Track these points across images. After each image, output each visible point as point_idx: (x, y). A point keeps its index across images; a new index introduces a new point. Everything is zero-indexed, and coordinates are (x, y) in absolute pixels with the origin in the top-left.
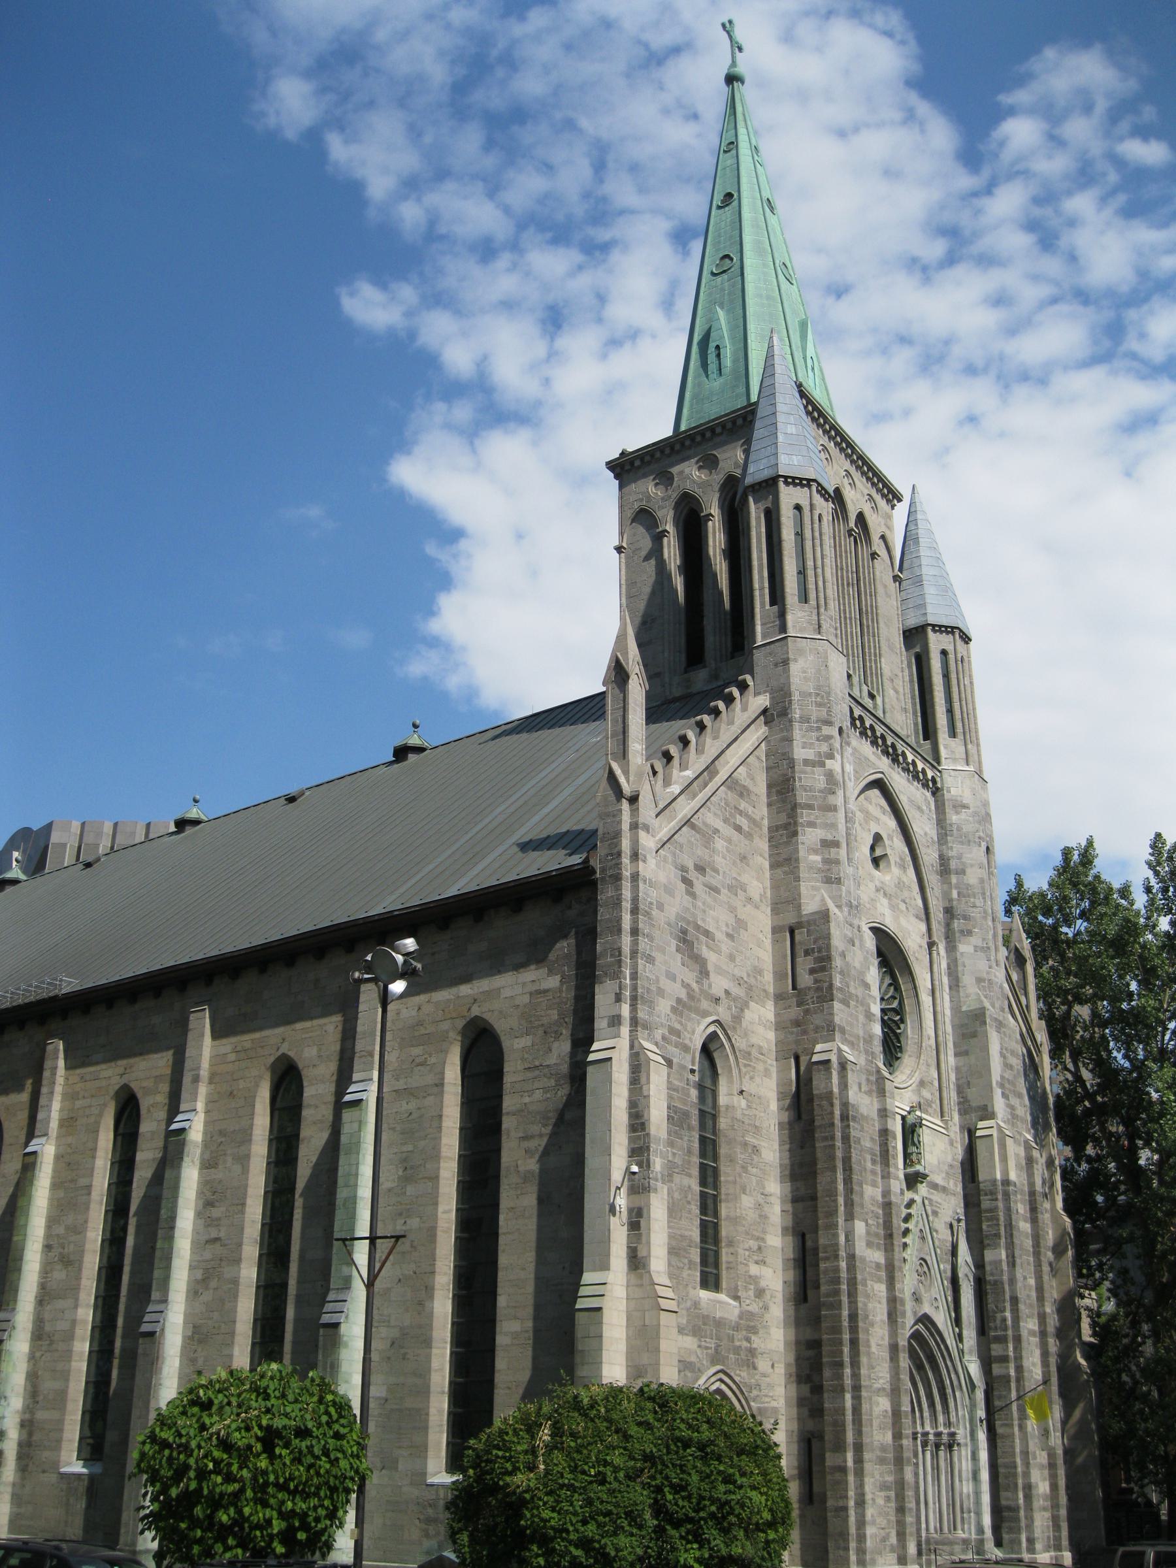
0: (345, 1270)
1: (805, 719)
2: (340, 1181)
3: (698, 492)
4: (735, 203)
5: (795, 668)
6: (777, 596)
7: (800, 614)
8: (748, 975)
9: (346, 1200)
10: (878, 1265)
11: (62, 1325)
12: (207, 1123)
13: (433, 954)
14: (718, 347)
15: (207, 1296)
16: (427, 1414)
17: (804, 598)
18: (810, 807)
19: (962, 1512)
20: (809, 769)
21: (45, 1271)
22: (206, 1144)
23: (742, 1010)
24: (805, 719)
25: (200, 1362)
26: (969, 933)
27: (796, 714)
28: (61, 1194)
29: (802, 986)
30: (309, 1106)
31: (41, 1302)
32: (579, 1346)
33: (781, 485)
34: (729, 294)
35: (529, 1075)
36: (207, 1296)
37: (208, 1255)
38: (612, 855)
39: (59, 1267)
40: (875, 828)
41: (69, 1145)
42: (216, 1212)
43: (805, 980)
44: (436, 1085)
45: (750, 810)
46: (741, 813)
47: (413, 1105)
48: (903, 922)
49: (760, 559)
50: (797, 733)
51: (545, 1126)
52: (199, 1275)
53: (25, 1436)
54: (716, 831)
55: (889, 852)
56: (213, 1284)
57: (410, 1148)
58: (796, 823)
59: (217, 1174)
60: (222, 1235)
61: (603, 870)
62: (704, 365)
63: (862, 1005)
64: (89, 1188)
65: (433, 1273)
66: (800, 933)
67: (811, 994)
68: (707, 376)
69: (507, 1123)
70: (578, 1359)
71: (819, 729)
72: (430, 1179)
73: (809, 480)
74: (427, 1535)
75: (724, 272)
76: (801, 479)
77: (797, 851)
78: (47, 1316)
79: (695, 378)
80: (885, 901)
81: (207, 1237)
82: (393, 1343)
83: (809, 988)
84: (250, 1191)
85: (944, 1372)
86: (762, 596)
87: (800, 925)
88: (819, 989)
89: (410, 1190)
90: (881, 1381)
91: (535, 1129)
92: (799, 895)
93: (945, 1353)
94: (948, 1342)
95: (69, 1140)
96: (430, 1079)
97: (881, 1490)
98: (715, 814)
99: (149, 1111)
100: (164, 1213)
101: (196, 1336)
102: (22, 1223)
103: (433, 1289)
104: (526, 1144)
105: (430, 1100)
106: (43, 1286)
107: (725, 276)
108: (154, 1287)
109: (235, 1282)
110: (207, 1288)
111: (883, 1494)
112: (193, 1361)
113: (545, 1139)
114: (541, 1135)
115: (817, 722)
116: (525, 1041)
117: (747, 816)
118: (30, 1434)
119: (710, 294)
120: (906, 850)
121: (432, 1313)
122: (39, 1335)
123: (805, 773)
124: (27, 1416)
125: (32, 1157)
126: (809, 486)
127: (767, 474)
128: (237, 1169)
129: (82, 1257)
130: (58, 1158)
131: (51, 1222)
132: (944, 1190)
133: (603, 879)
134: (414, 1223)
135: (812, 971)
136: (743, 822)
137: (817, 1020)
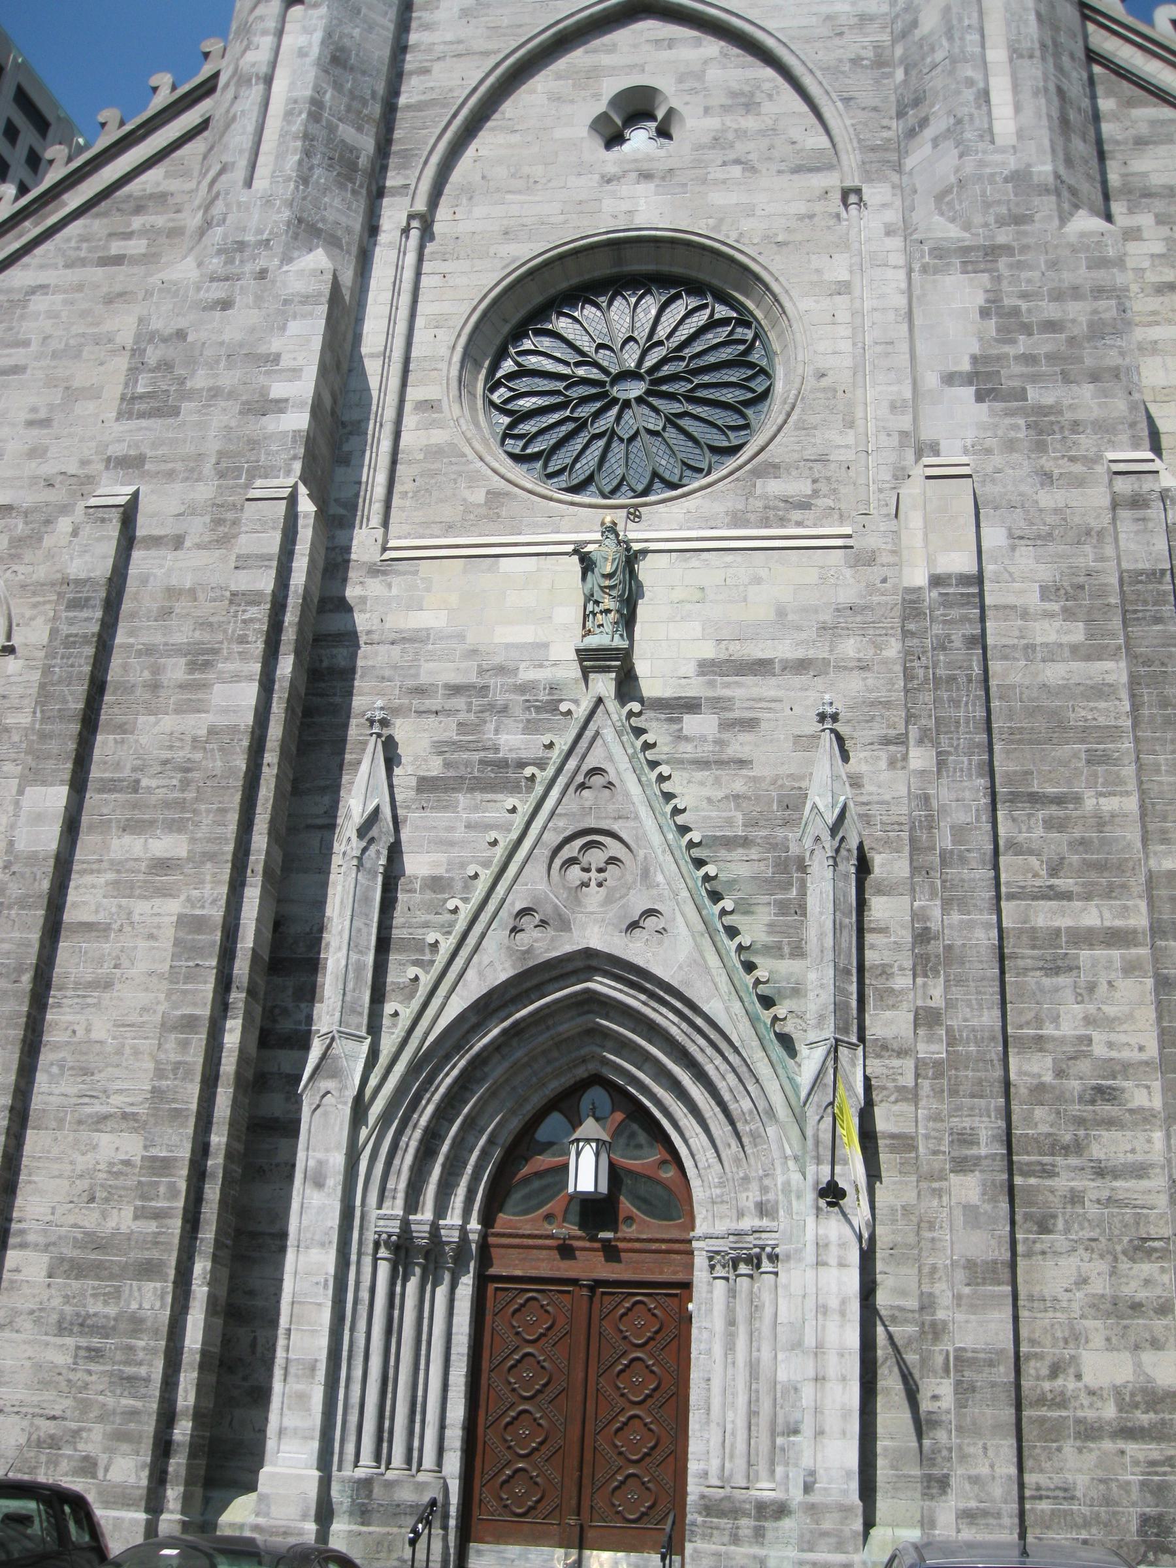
8: (84, 463)
10: (163, 865)
19: (773, 1434)
23: (48, 522)
26: (924, 122)
40: (612, 86)
45: (160, 221)
46: (128, 236)
48: (718, 198)
54: (43, 288)
55: (675, 103)
63: (231, 395)
80: (645, 189)
85: (726, 1083)
90: (117, 1100)
93: (713, 1035)
94: (713, 1007)
97: (62, 1329)
98: (42, 267)
111: (70, 1341)
120: (769, 72)
132: (801, 666)
136: (136, 246)
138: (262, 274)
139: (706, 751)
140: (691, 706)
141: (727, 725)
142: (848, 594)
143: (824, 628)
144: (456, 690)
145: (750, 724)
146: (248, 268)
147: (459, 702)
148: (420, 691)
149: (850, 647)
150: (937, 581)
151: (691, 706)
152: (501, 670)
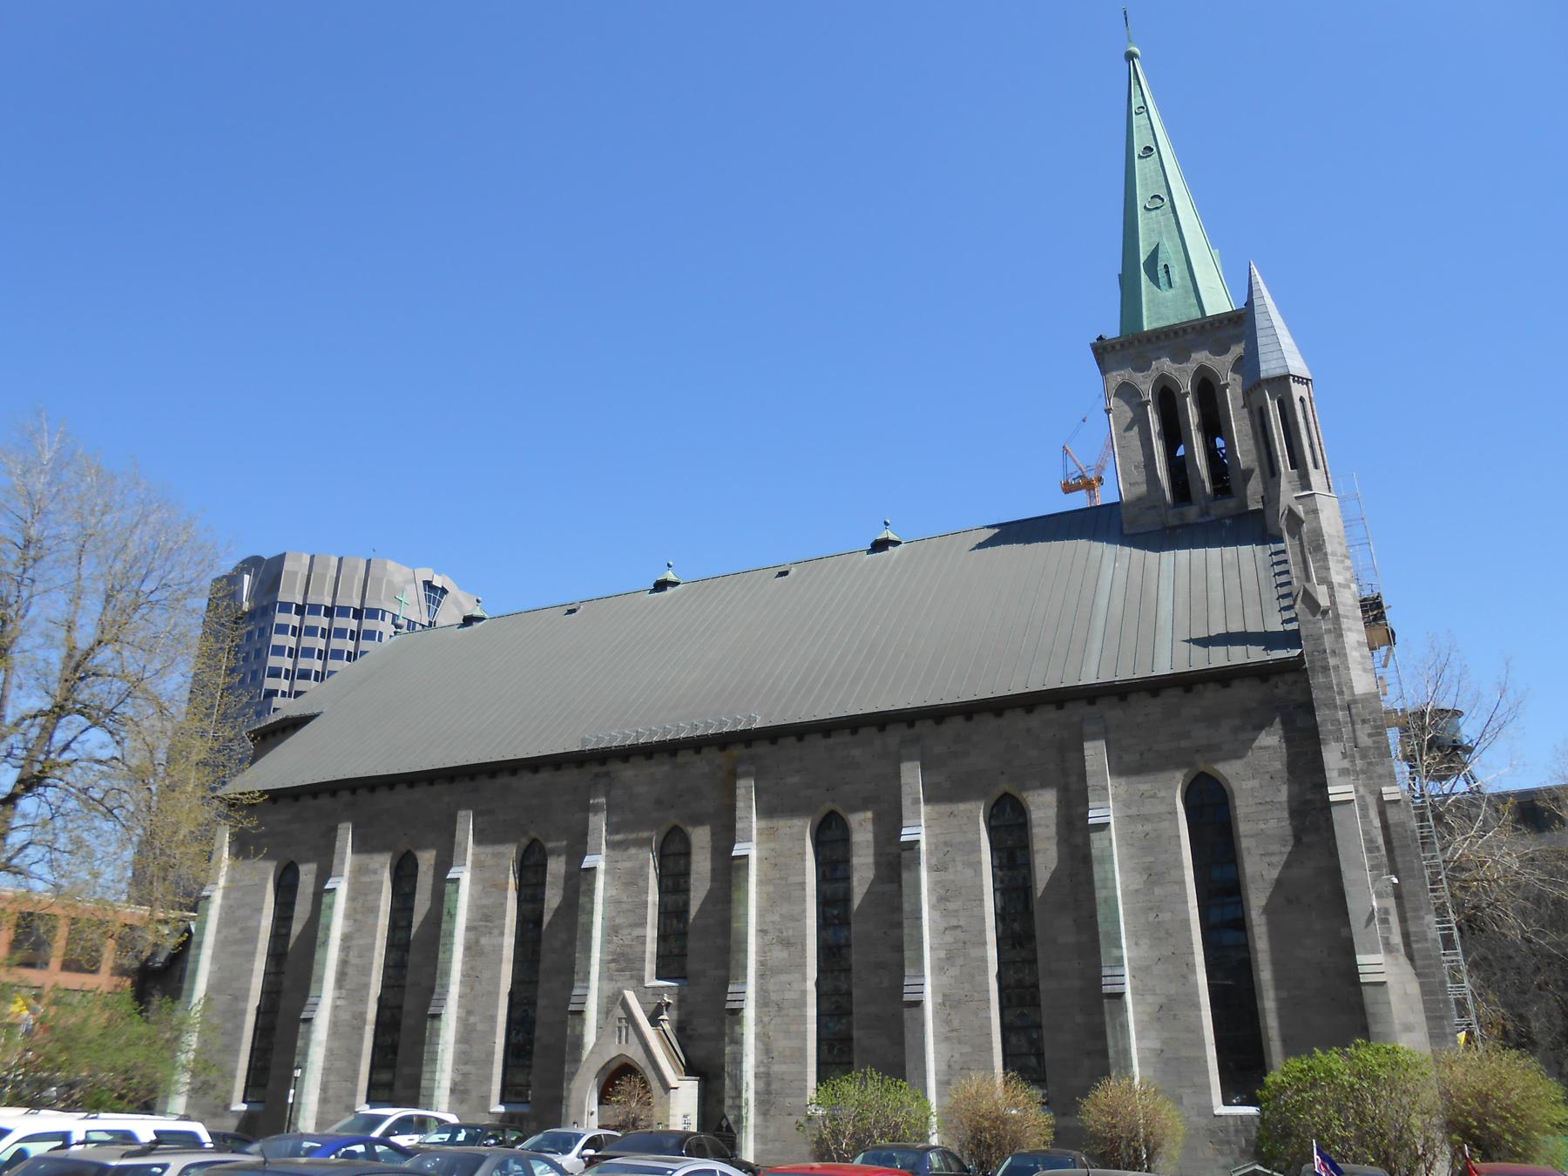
0: (1115, 952)
1: (1334, 554)
2: (1097, 884)
3: (1175, 375)
4: (1155, 155)
5: (1322, 516)
6: (1297, 461)
7: (1317, 477)
9: (1106, 900)
11: (789, 995)
12: (928, 837)
13: (1147, 715)
14: (1166, 266)
15: (954, 971)
16: (1206, 1061)
17: (1316, 467)
18: (1347, 617)
20: (1342, 590)
21: (763, 951)
22: (930, 853)
24: (1334, 554)
25: (956, 1024)
27: (1329, 549)
28: (771, 889)
29: (1363, 745)
30: (1039, 825)
31: (761, 976)
32: (1370, 1009)
33: (1291, 380)
34: (1166, 225)
35: (1261, 808)
36: (954, 971)
37: (949, 938)
38: (1318, 652)
39: (779, 947)
41: (773, 850)
42: (951, 906)
43: (1364, 740)
44: (1170, 813)
47: (1148, 827)
49: (1279, 434)
50: (1332, 564)
51: (1284, 846)
52: (942, 954)
53: (762, 1085)
56: (960, 961)
57: (1152, 859)
58: (1341, 629)
59: (948, 876)
60: (961, 923)
61: (1311, 662)
62: (1154, 278)
64: (803, 885)
65: (1193, 953)
66: (1356, 707)
67: (1372, 751)
68: (1159, 287)
69: (1245, 843)
70: (1370, 1020)
71: (1342, 562)
72: (1176, 883)
73: (1307, 380)
74: (1221, 1153)
75: (1157, 208)
76: (1303, 378)
77: (1344, 648)
78: (771, 987)
79: (1147, 287)
81: (946, 925)
82: (1161, 1007)
83: (1370, 747)
84: (985, 890)
86: (1284, 461)
87: (1355, 701)
88: (1378, 748)
89: (1157, 891)
91: (1275, 848)
92: (1351, 680)
95: (772, 845)
96: (1162, 808)
99: (861, 824)
100: (907, 906)
101: (948, 1004)
102: (741, 911)
103: (1194, 965)
104: (1267, 859)
105: (1165, 824)
106: (762, 964)
107: (1158, 211)
108: (907, 963)
109: (984, 960)
110: (953, 965)
112: (948, 1022)
113: (1285, 857)
114: (1281, 853)
115: (1341, 556)
116: (1255, 783)
118: (768, 1084)
119: (1147, 224)
121: (1197, 984)
122: (763, 1002)
123: (1339, 592)
124: (762, 1069)
125: (742, 861)
126: (1307, 384)
127: (1279, 372)
128: (969, 873)
129: (805, 939)
130: (760, 860)
131: (761, 914)
133: (1313, 669)
134: (1166, 916)
135: (1370, 735)
137: (1380, 770)
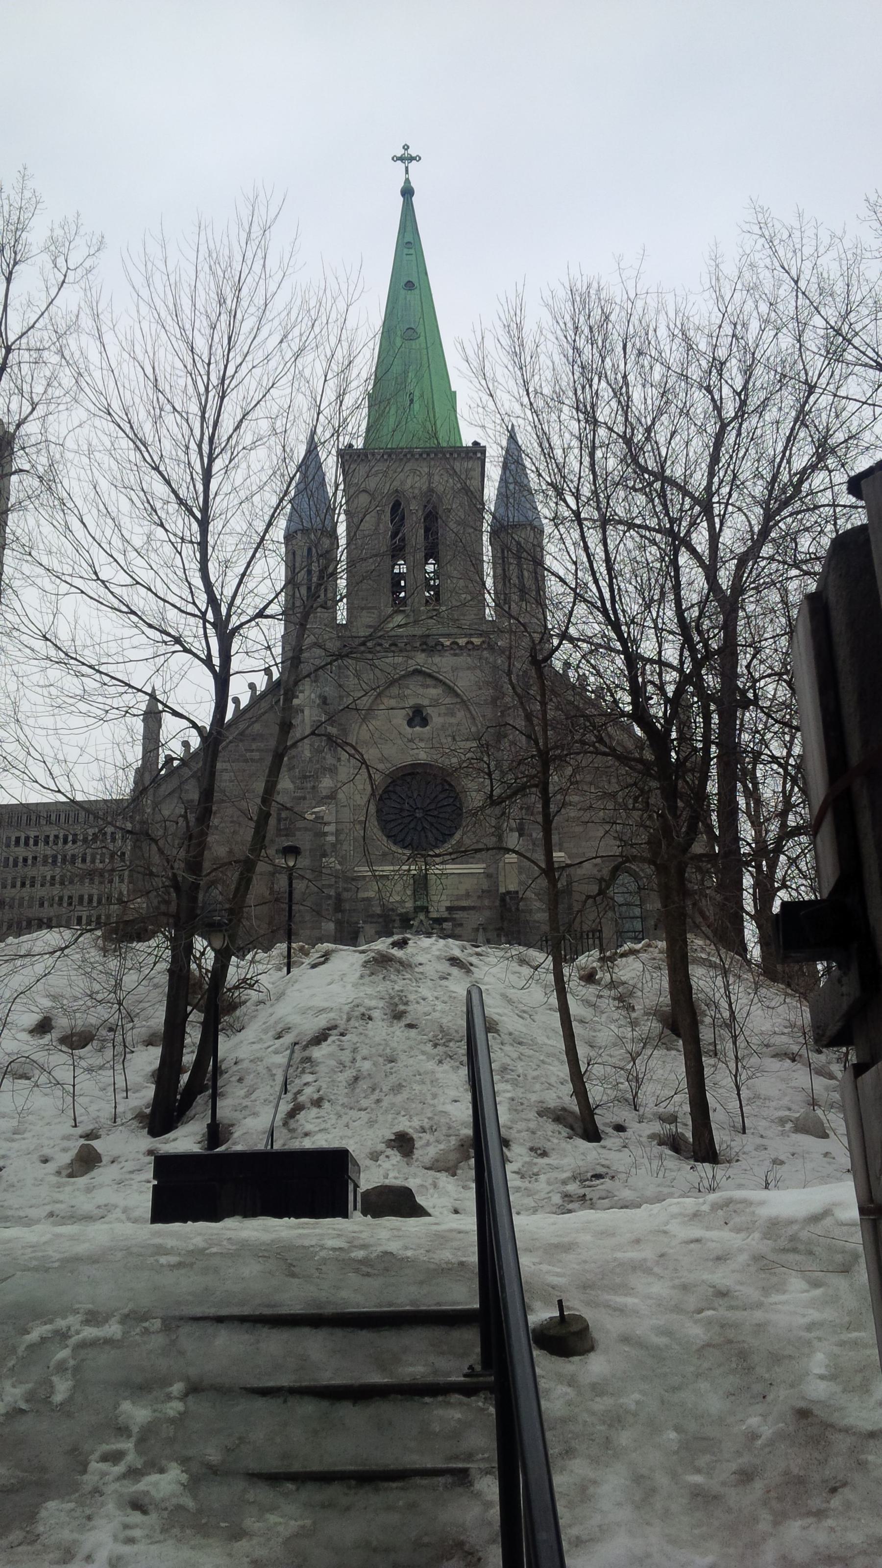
45: (262, 745)
46: (252, 751)
117: (258, 750)
138: (314, 787)
139: (449, 932)
140: (446, 920)
141: (454, 926)
142: (485, 887)
143: (479, 897)
144: (379, 916)
145: (461, 925)
146: (309, 785)
147: (381, 920)
148: (372, 916)
149: (486, 902)
150: (509, 893)
151: (446, 920)
152: (393, 910)
